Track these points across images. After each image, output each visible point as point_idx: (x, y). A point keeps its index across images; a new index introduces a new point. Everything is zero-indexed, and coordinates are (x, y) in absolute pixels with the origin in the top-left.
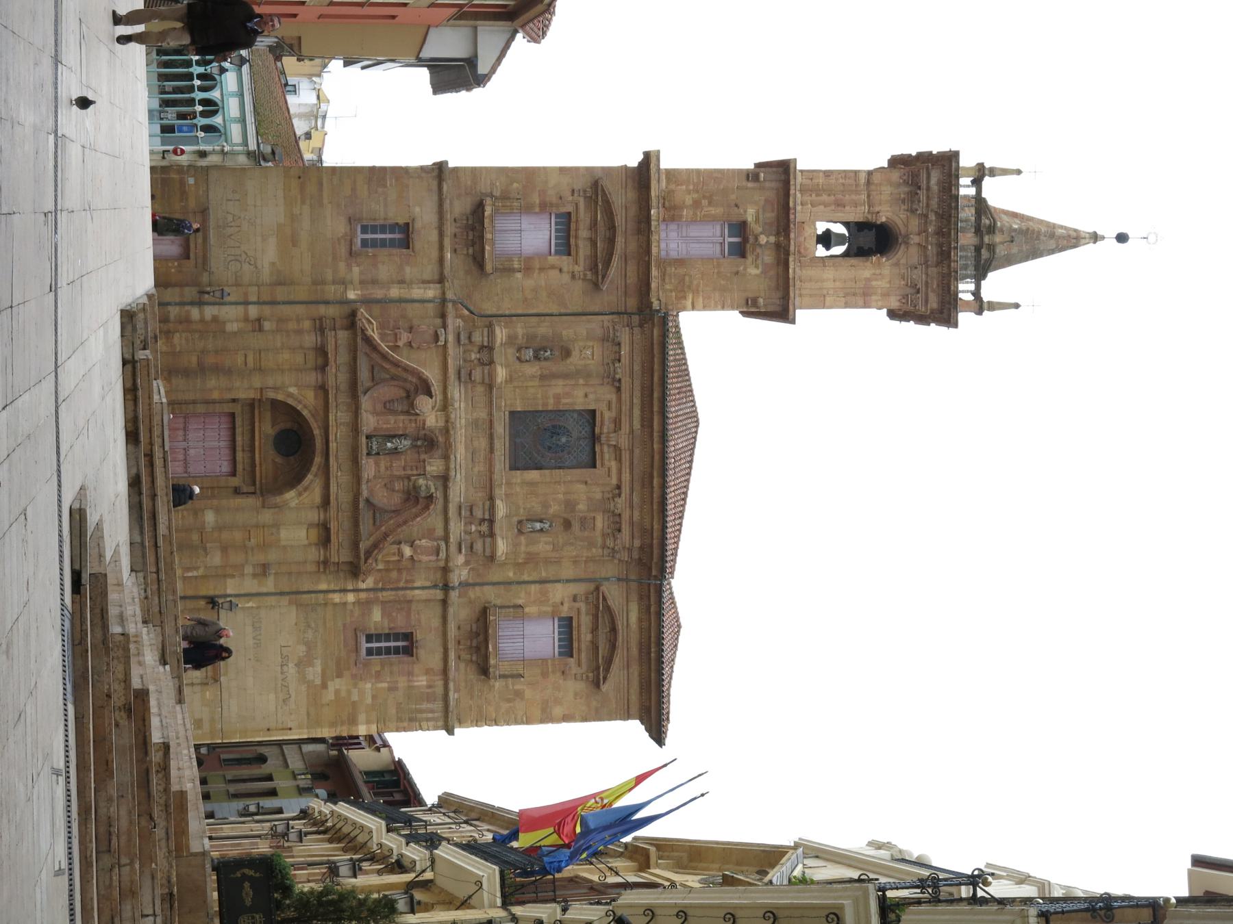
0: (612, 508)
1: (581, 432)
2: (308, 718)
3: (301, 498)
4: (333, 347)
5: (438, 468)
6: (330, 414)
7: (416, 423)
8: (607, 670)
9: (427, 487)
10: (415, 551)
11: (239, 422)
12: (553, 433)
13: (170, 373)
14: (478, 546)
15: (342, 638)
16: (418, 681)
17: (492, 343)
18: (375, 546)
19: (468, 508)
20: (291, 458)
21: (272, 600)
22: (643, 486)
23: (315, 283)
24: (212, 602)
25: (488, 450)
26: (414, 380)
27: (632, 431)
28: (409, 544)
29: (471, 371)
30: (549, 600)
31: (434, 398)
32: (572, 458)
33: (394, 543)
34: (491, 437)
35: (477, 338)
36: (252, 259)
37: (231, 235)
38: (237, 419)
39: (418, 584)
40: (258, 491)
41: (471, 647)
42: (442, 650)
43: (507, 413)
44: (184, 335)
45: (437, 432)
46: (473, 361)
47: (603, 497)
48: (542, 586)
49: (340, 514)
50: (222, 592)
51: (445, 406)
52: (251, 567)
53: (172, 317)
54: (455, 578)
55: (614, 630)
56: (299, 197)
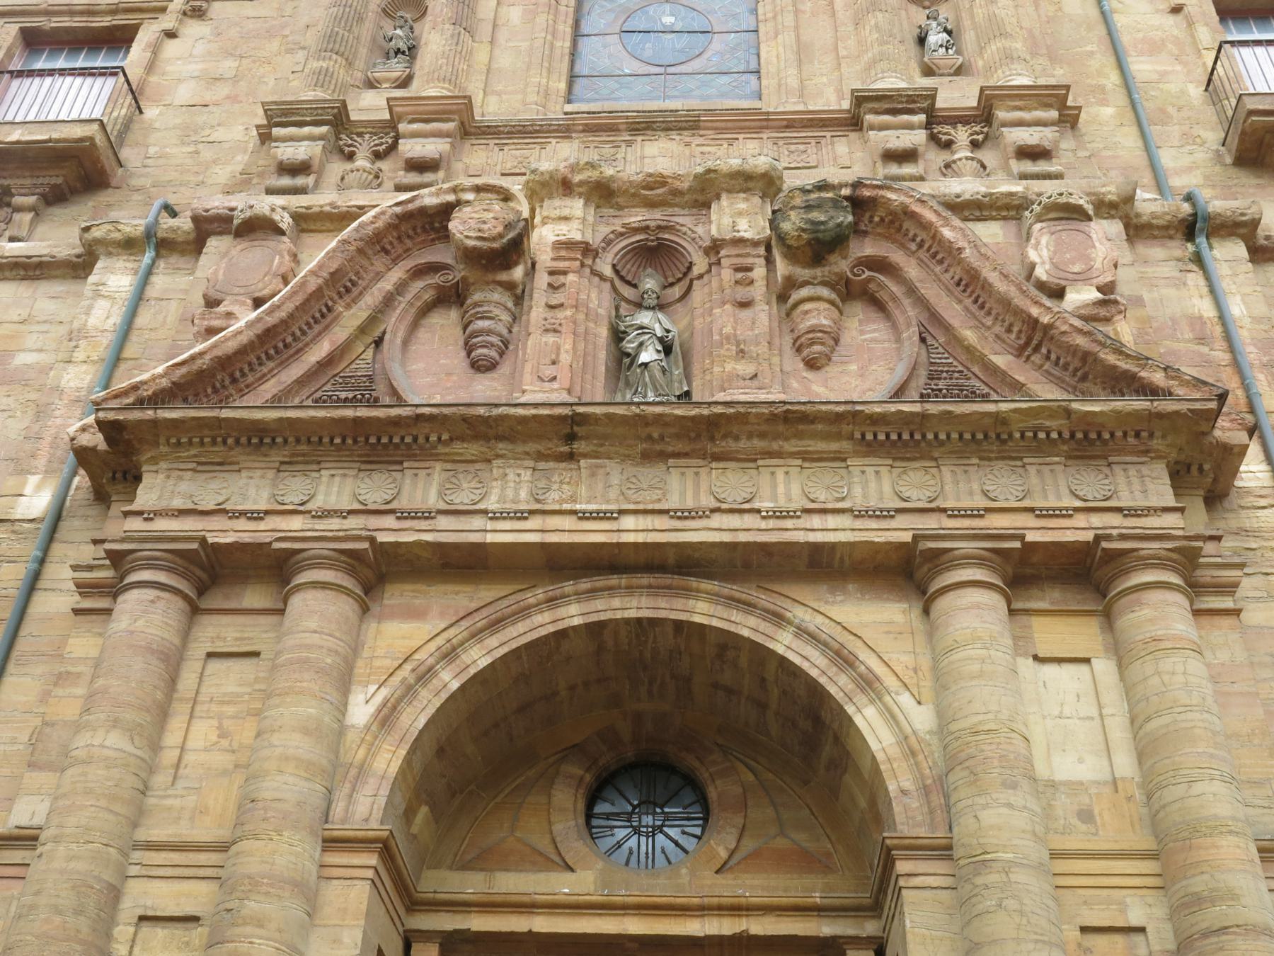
3: (890, 681)
5: (740, 214)
6: (490, 538)
7: (564, 273)
10: (1082, 278)
26: (396, 274)
39: (1206, 308)
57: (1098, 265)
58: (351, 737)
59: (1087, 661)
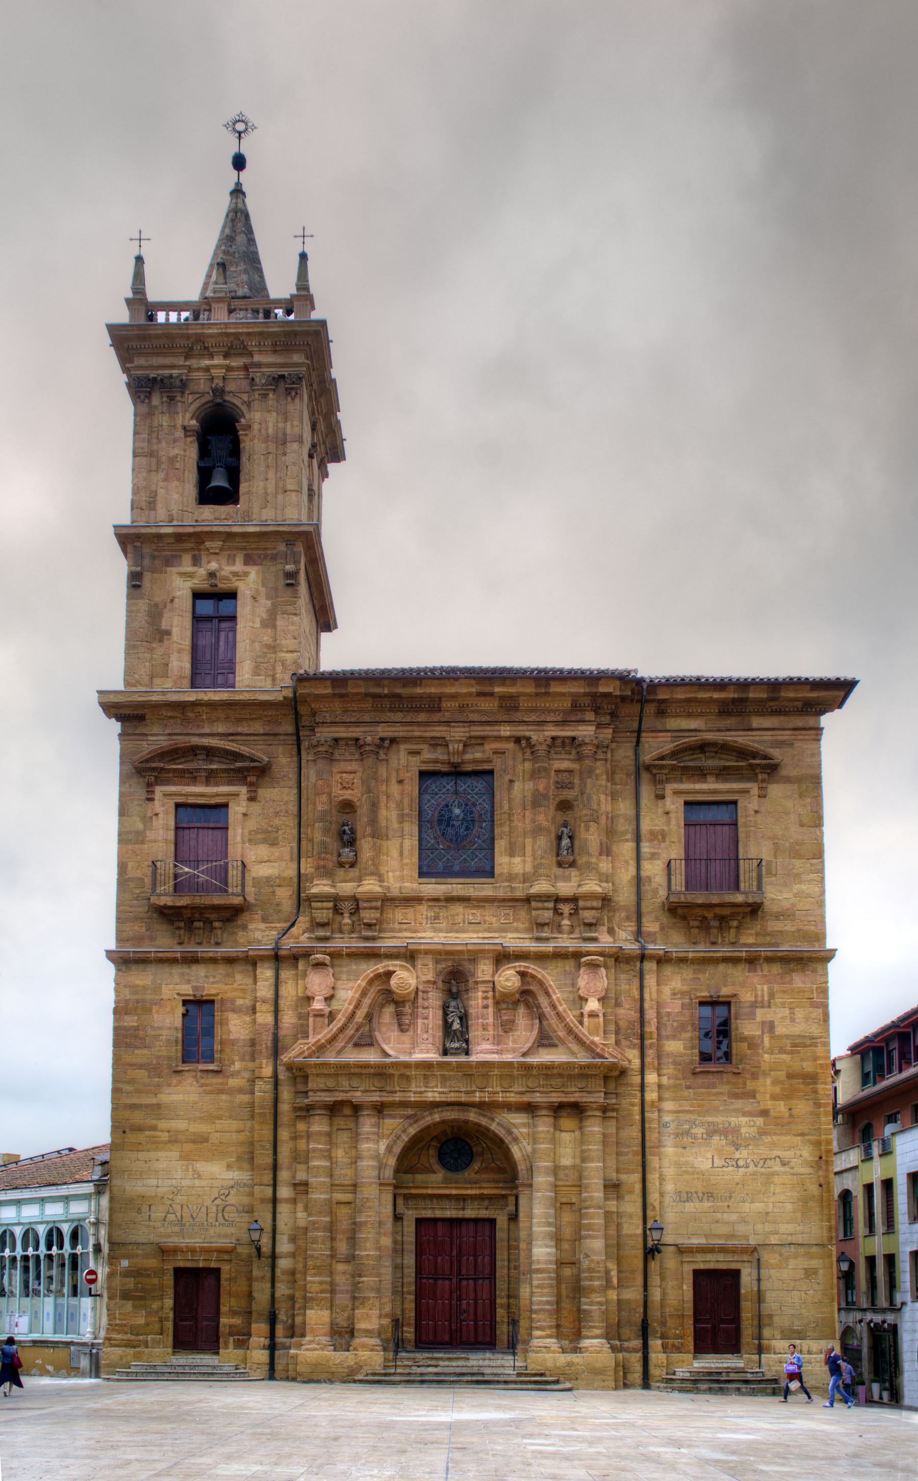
0: (544, 747)
1: (448, 790)
2: (807, 1135)
4: (327, 1094)
8: (754, 755)
12: (448, 825)
14: (588, 916)
15: (703, 1090)
16: (763, 996)
17: (330, 897)
20: (474, 1150)
21: (653, 1178)
22: (516, 709)
23: (252, 1117)
24: (651, 1252)
25: (465, 904)
27: (447, 723)
29: (365, 924)
30: (663, 830)
32: (480, 801)
33: (581, 1023)
34: (451, 900)
35: (323, 915)
36: (222, 1192)
37: (192, 1216)
38: (424, 1216)
40: (514, 1192)
41: (720, 928)
42: (724, 964)
43: (421, 880)
44: (309, 1278)
45: (440, 967)
46: (353, 922)
47: (529, 760)
48: (643, 837)
50: (640, 1240)
51: (410, 956)
53: (288, 1292)
54: (632, 947)
55: (703, 747)
56: (147, 1133)
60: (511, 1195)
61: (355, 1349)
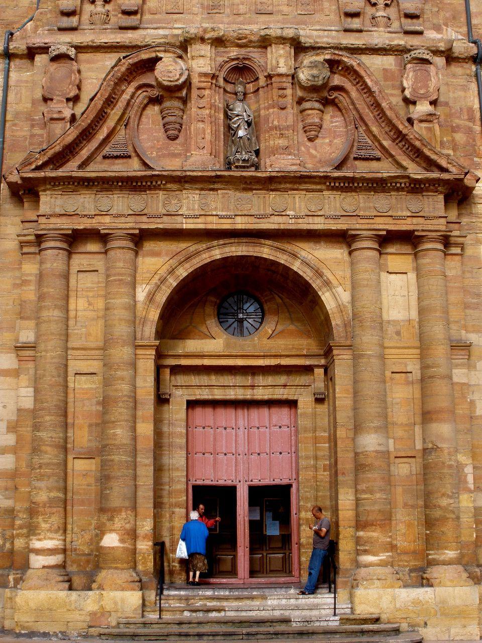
6: (185, 227)
9: (313, 65)
10: (424, 97)
11: (204, 394)
13: (102, 510)
18: (417, 154)
19: (349, 20)
26: (130, 90)
28: (411, 107)
31: (160, 55)
38: (198, 397)
45: (220, 60)
49: (361, 213)
52: (455, 371)
57: (431, 90)
58: (140, 306)
59: (406, 273)
60: (318, 366)
61: (101, 588)
